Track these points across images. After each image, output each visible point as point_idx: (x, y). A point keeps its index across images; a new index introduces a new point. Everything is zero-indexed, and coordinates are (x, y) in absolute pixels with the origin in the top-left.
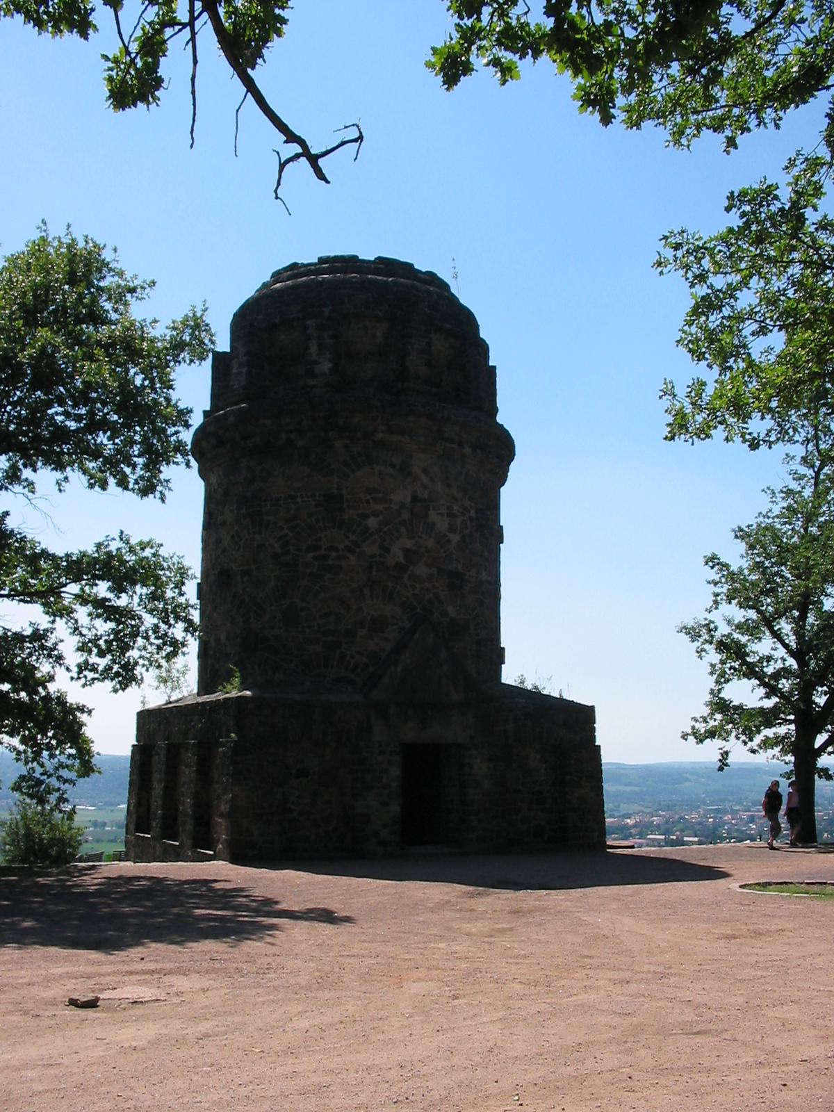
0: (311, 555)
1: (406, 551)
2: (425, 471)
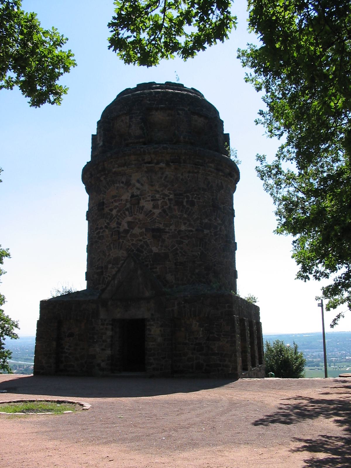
1: (129, 223)
2: (138, 181)
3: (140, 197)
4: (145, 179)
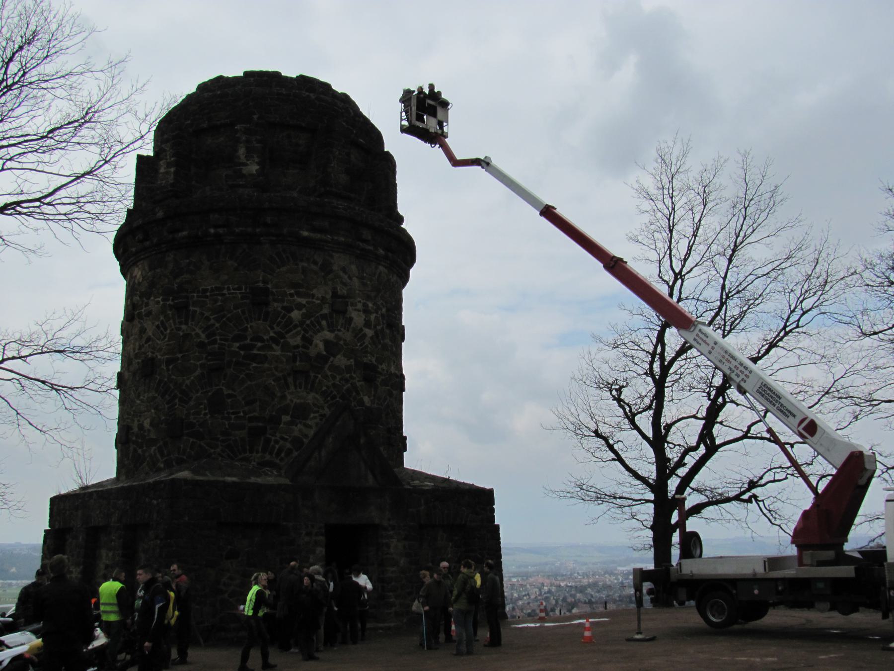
0: (237, 344)
1: (327, 343)
2: (344, 270)
4: (353, 267)
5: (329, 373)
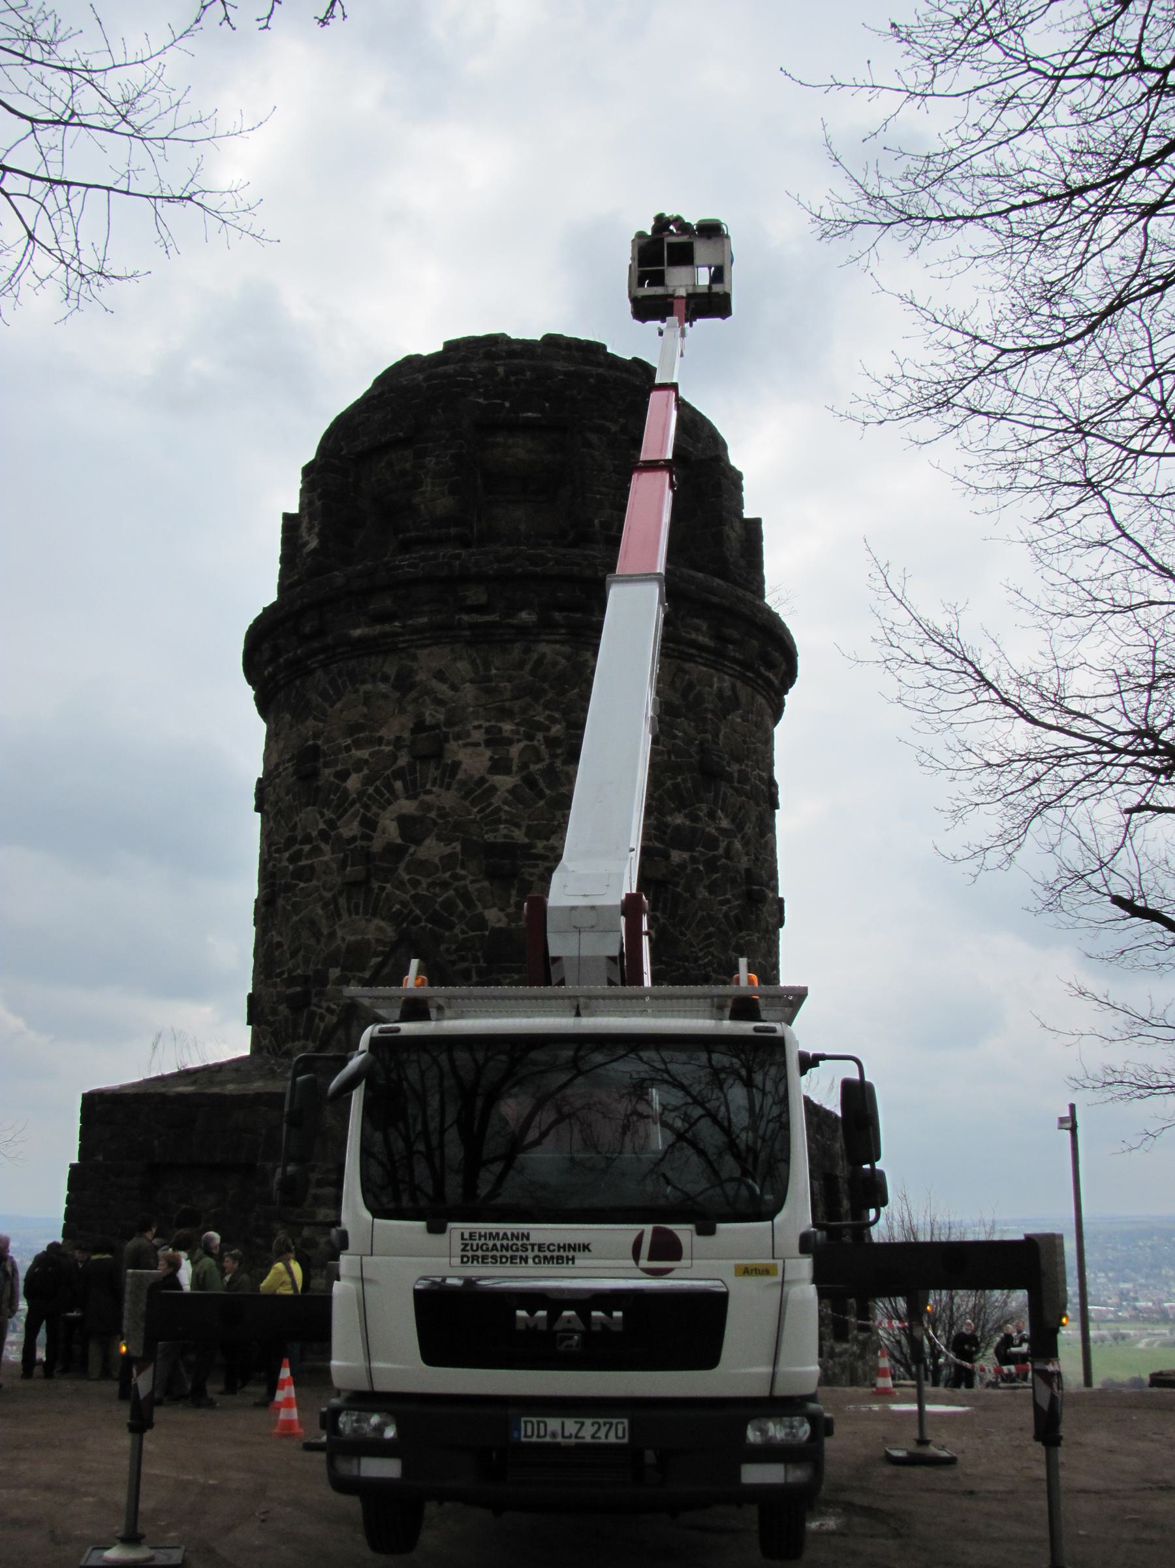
1: (403, 821)
2: (440, 676)
3: (444, 729)
4: (463, 666)
5: (406, 877)
